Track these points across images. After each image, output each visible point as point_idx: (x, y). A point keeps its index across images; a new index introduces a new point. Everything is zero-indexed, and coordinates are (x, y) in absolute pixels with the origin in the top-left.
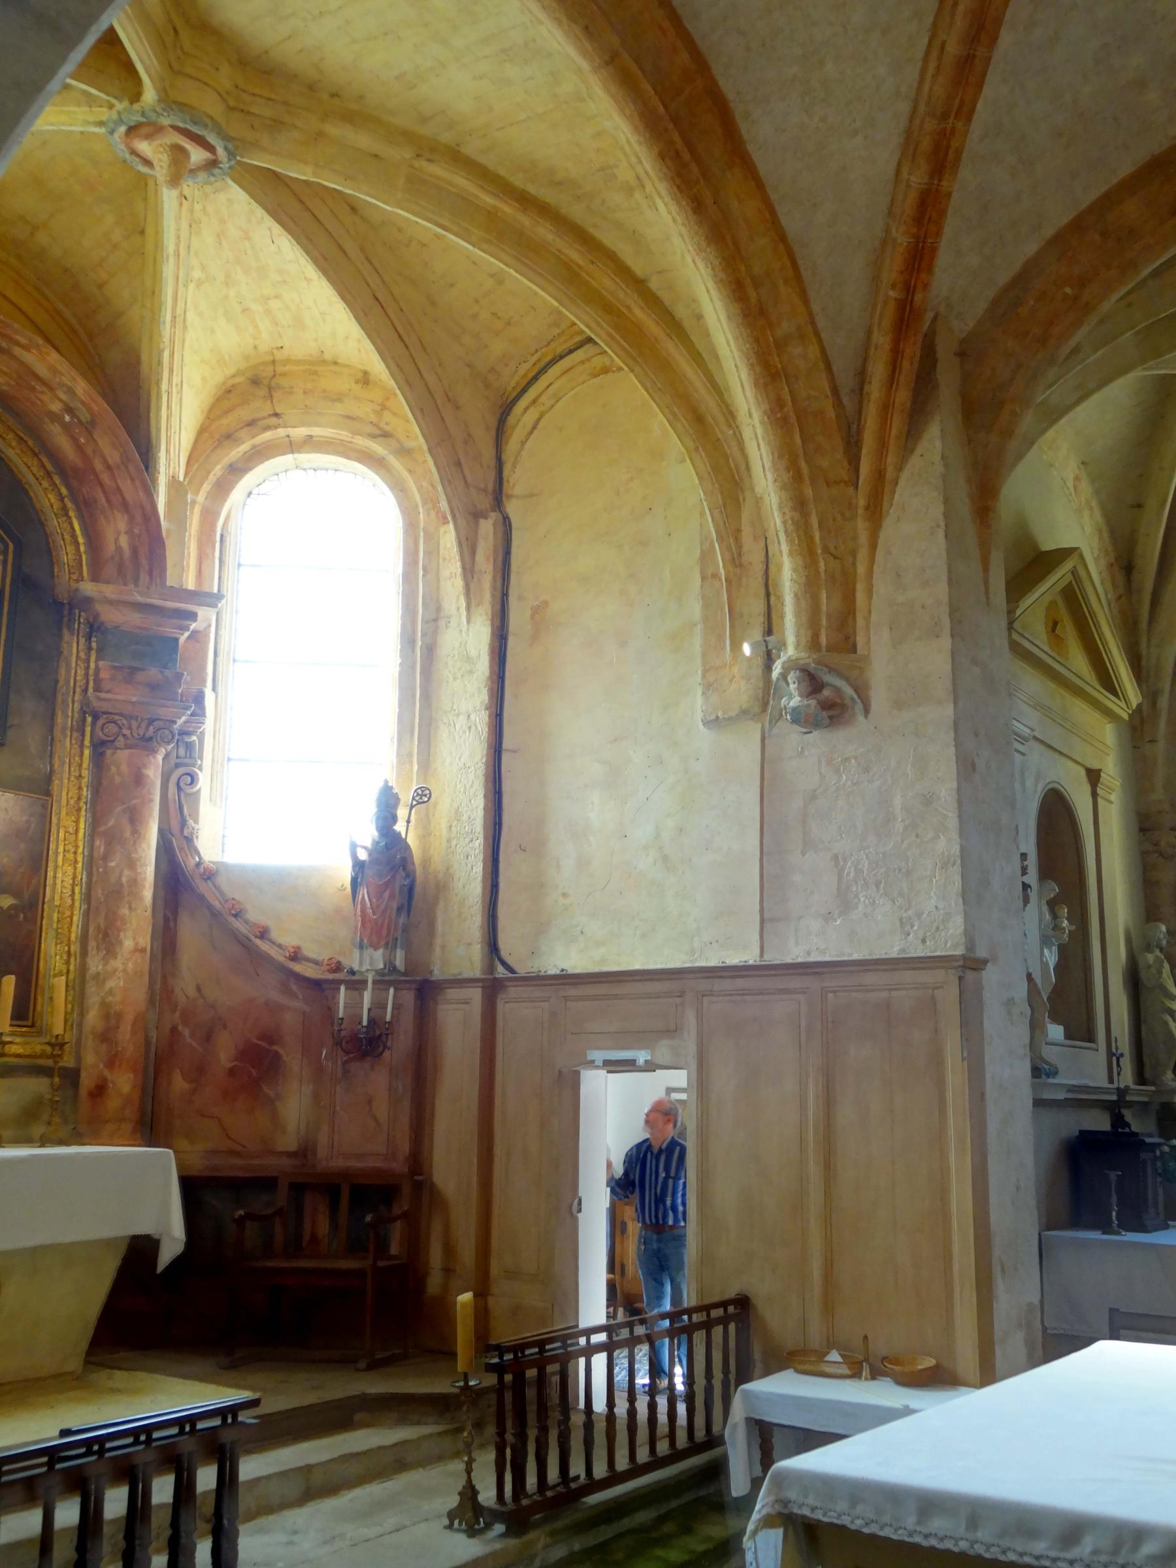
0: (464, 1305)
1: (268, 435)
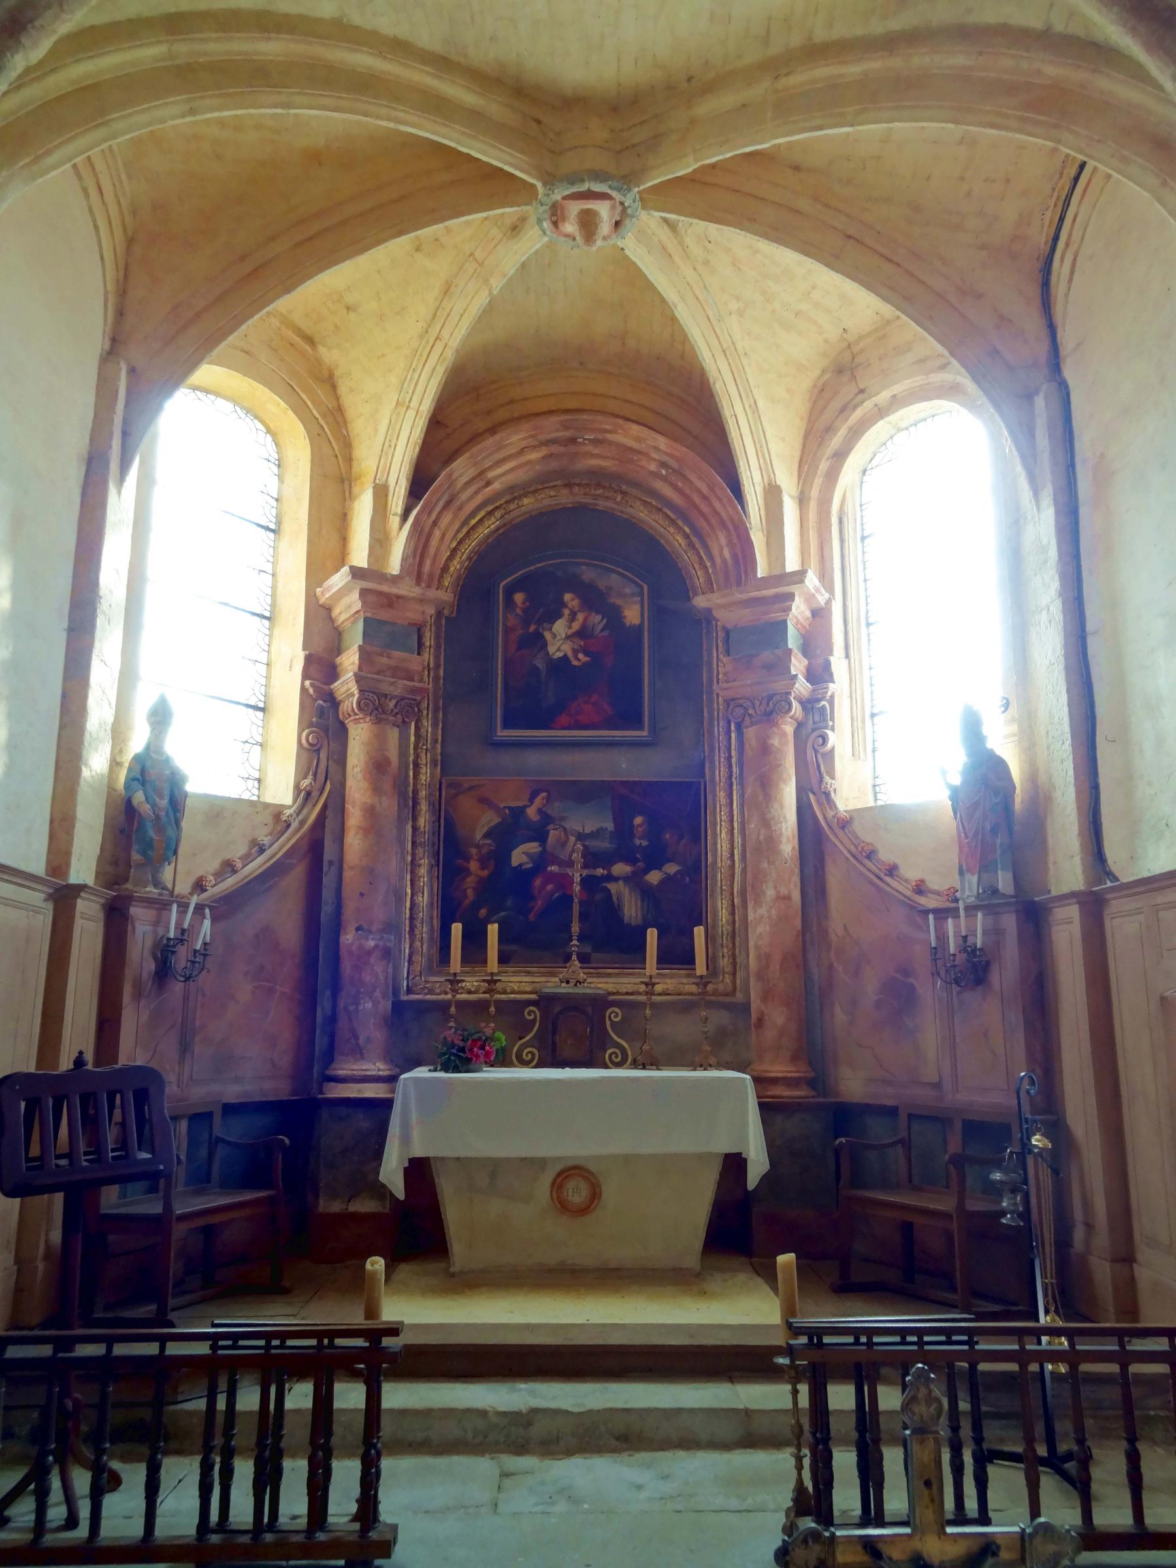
0: (787, 1265)
1: (858, 413)
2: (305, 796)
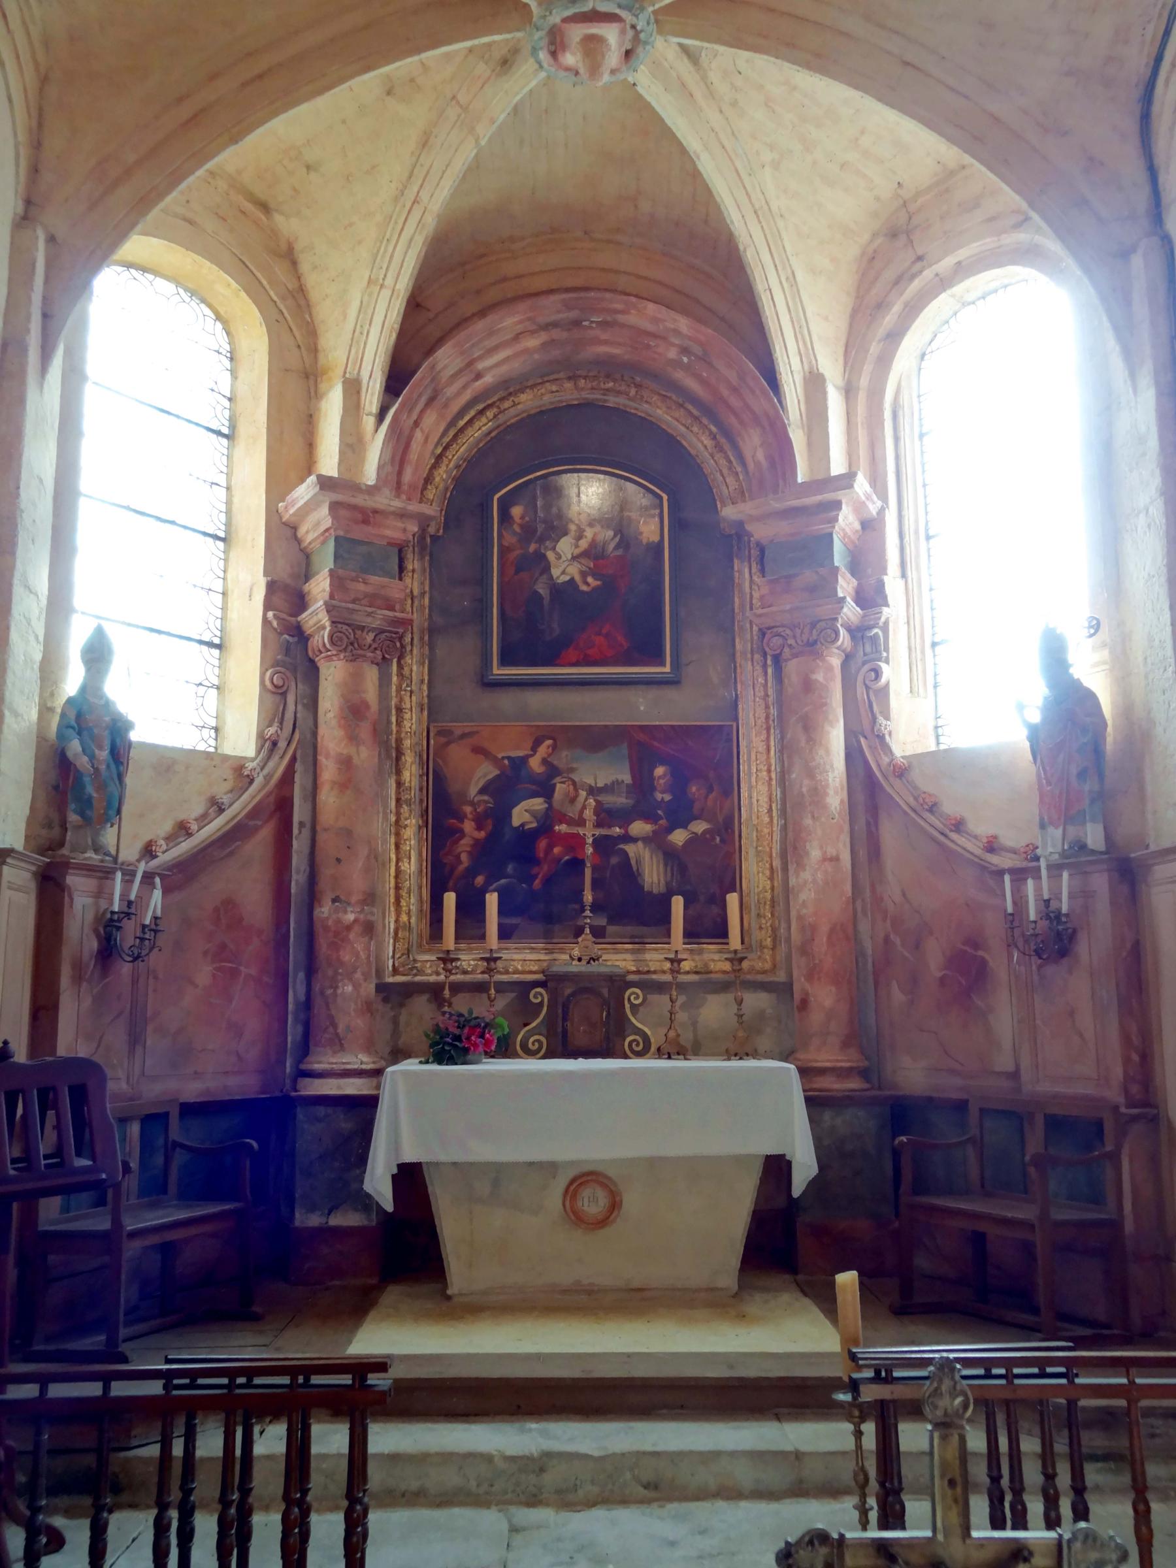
1: (916, 284)
2: (268, 745)
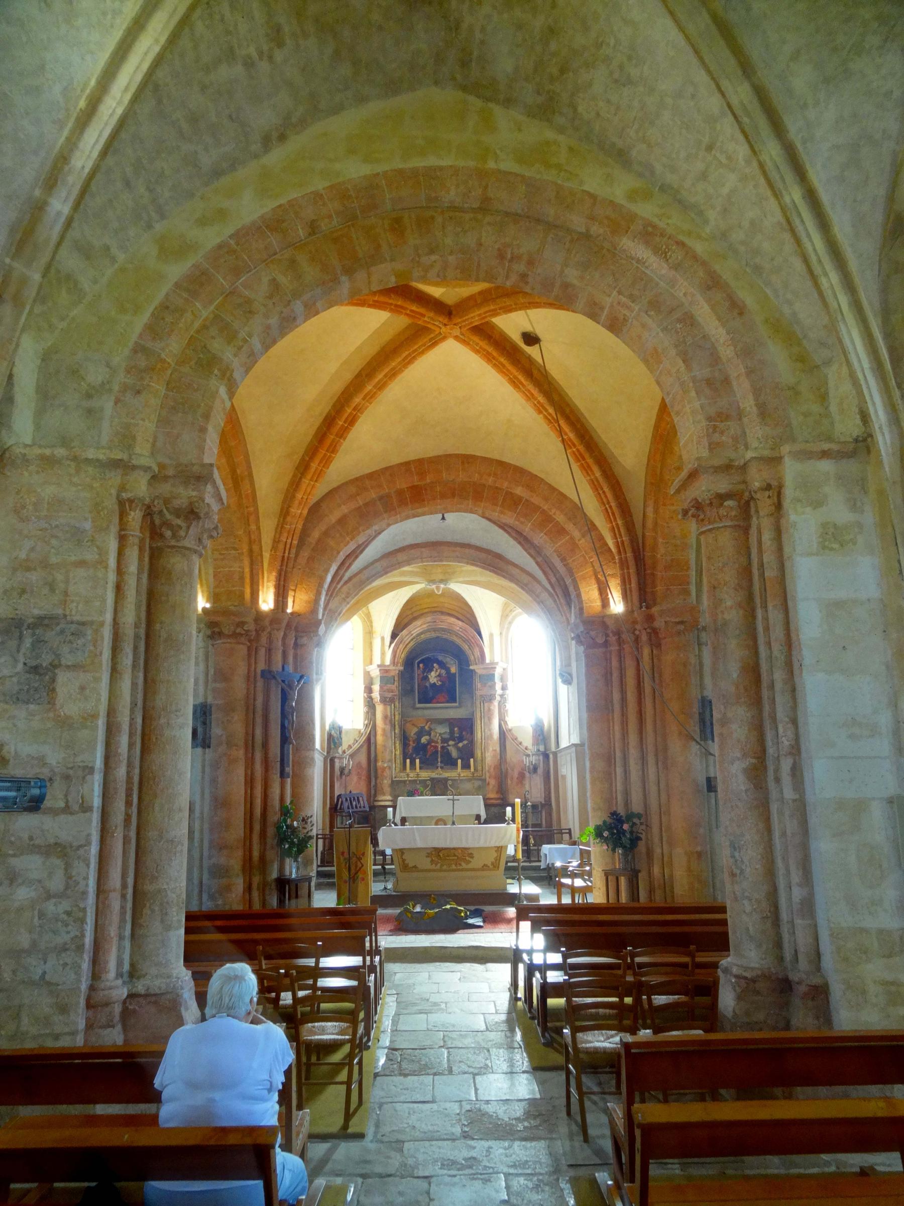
2: (367, 726)
